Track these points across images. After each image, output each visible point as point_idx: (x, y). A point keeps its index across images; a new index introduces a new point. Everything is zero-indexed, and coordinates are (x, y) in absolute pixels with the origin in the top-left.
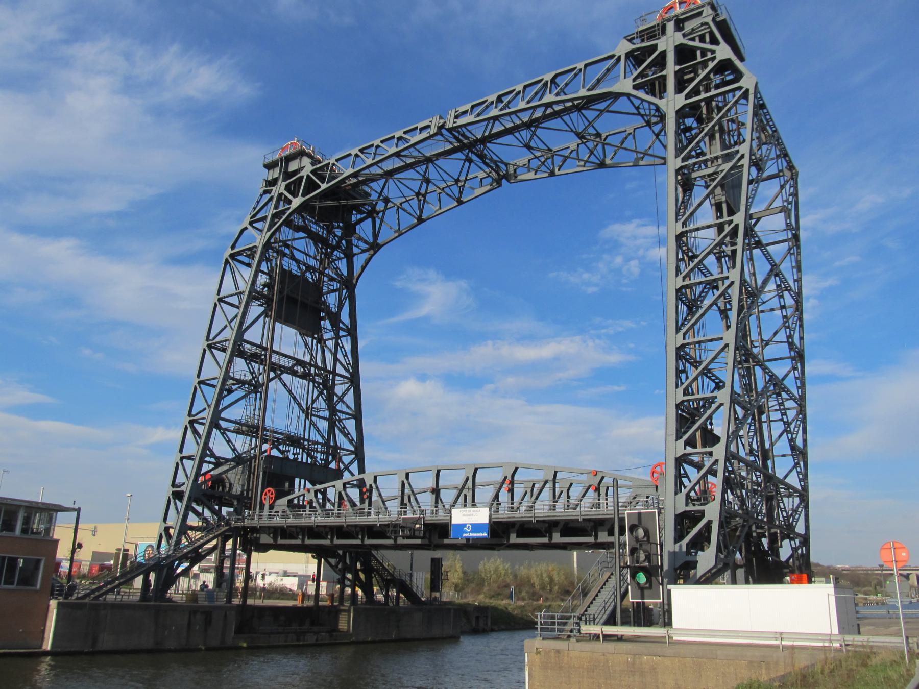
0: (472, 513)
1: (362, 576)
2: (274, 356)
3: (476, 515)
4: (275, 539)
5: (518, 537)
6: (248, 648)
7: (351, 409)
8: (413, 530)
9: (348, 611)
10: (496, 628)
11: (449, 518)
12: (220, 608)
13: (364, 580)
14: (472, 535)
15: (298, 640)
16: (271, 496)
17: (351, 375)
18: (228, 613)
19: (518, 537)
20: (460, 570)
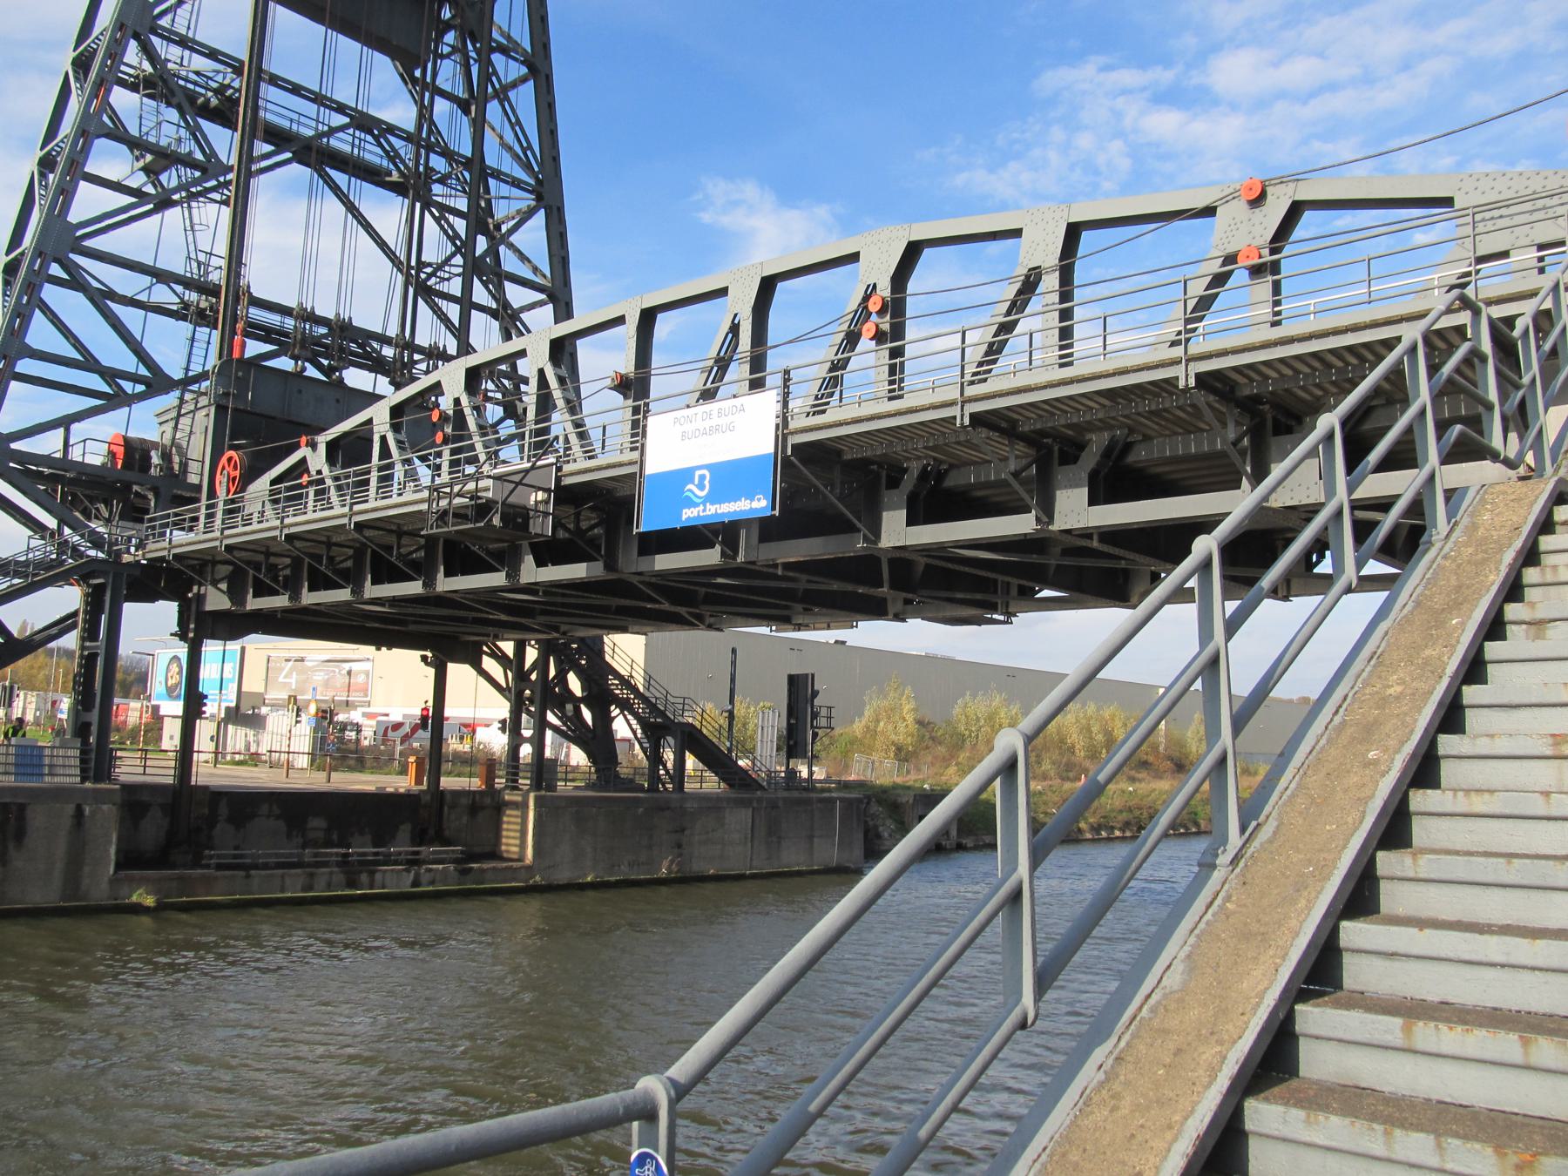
0: (715, 421)
1: (587, 715)
2: (269, 92)
3: (731, 428)
4: (236, 594)
5: (912, 521)
6: (161, 907)
7: (544, 276)
8: (517, 517)
9: (523, 806)
10: (969, 842)
11: (635, 455)
12: (59, 793)
13: (590, 722)
14: (712, 509)
15: (352, 884)
16: (233, 474)
17: (537, 179)
18: (87, 810)
19: (912, 521)
20: (910, 718)
